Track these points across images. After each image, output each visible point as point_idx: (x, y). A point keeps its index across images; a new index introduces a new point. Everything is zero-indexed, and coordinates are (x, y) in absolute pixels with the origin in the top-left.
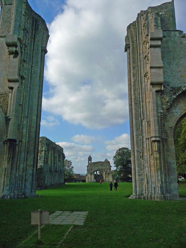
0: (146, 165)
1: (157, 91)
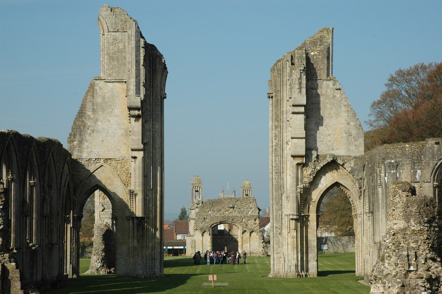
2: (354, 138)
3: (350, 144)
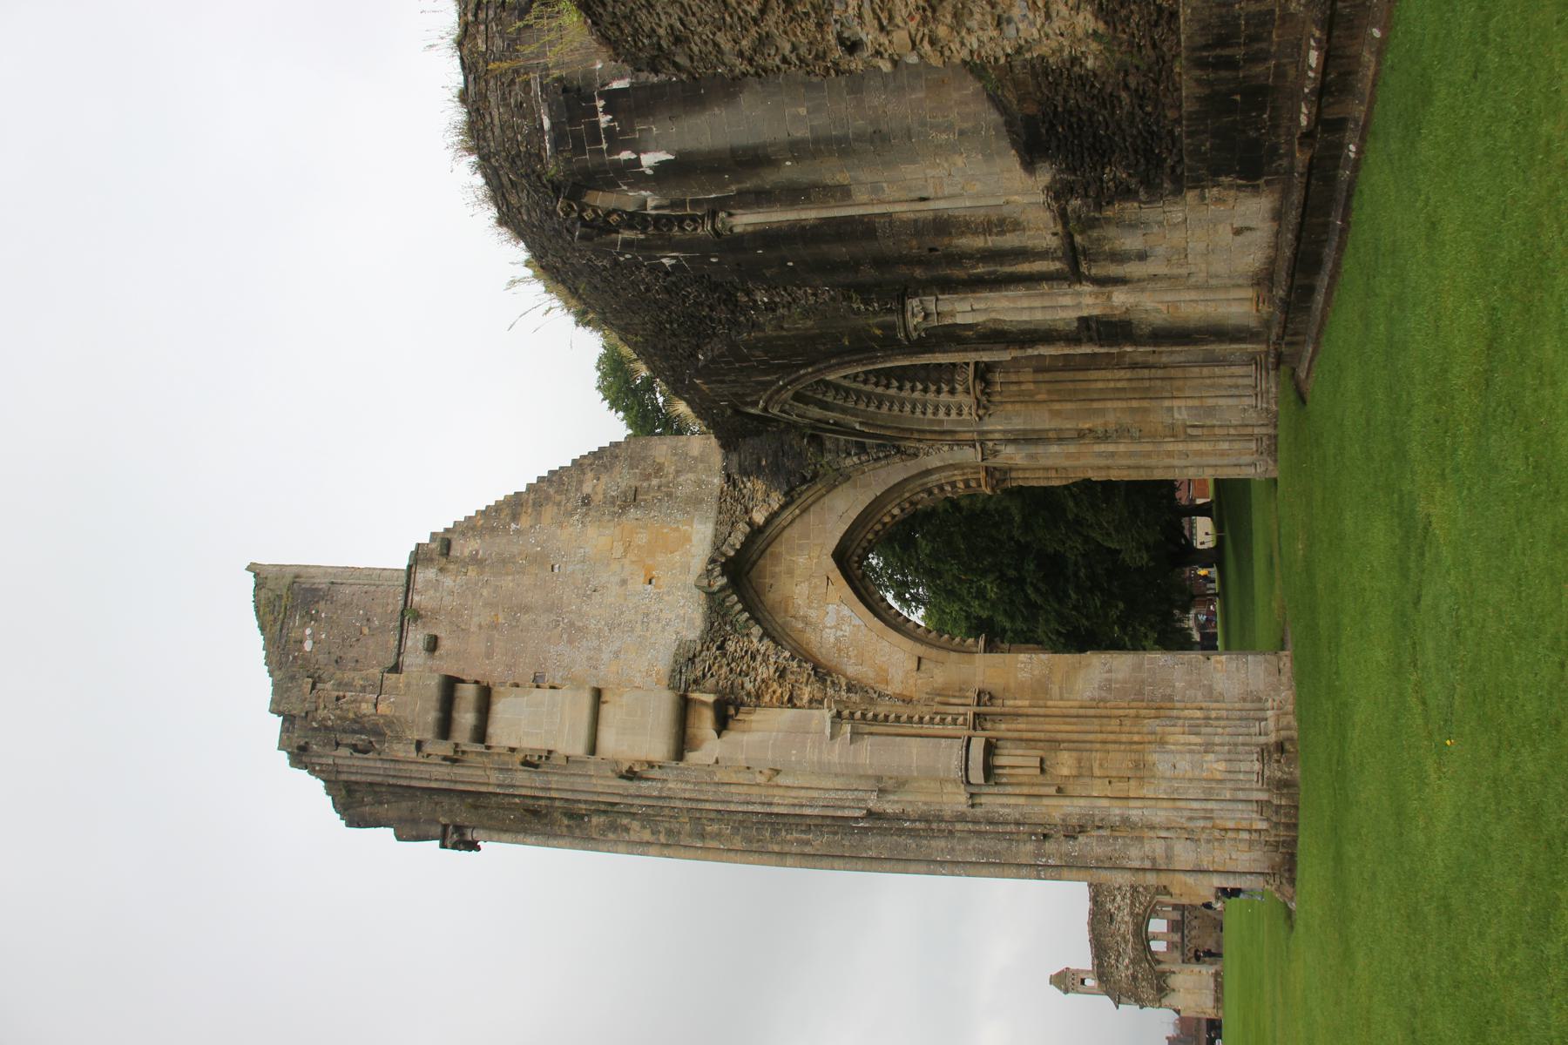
1: (722, 724)
2: (647, 477)
3: (669, 495)
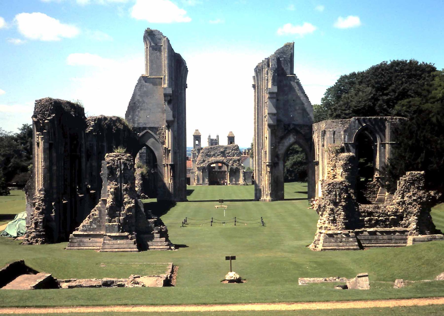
0: (263, 180)
